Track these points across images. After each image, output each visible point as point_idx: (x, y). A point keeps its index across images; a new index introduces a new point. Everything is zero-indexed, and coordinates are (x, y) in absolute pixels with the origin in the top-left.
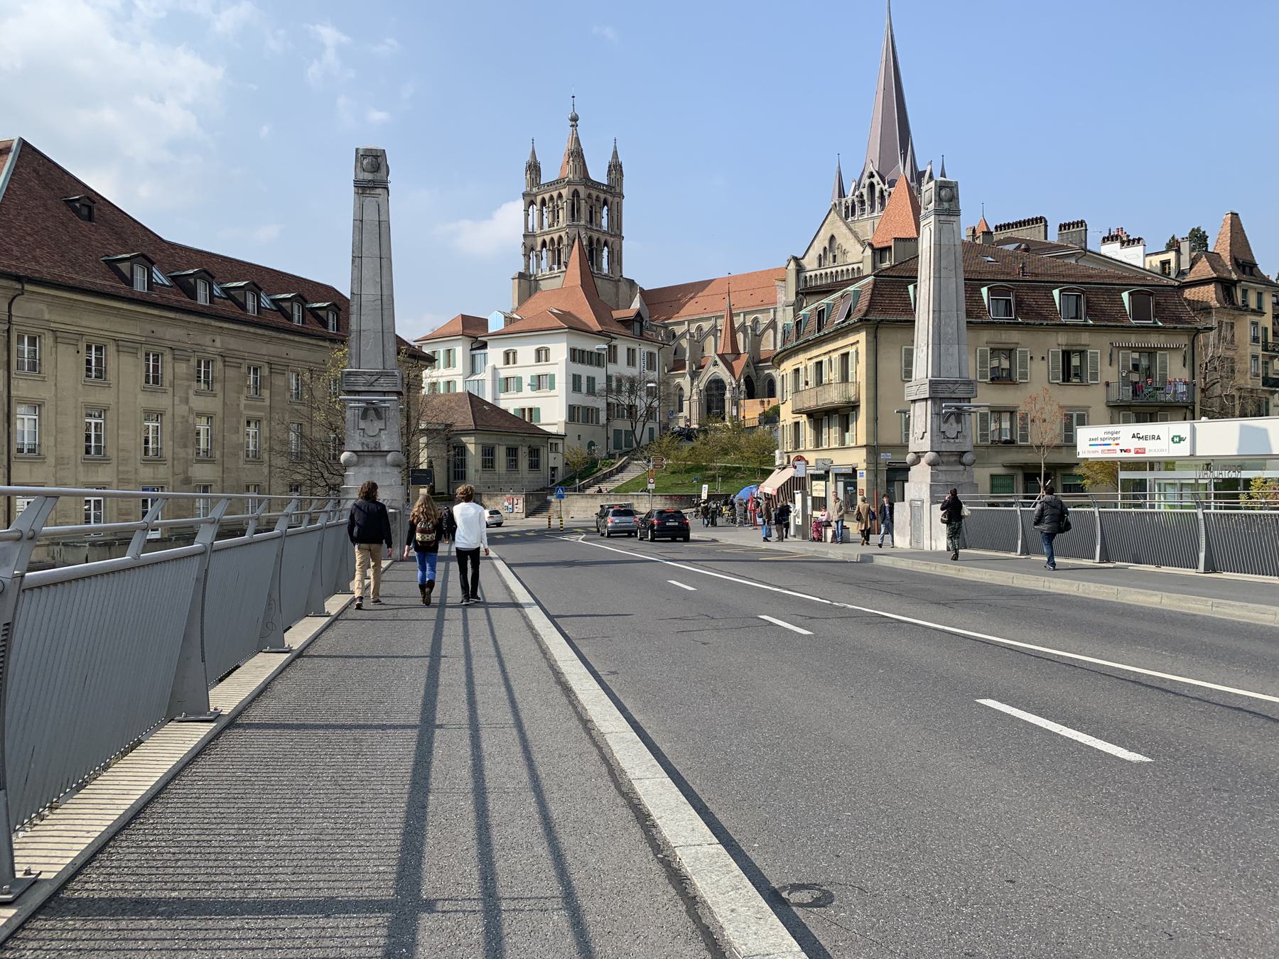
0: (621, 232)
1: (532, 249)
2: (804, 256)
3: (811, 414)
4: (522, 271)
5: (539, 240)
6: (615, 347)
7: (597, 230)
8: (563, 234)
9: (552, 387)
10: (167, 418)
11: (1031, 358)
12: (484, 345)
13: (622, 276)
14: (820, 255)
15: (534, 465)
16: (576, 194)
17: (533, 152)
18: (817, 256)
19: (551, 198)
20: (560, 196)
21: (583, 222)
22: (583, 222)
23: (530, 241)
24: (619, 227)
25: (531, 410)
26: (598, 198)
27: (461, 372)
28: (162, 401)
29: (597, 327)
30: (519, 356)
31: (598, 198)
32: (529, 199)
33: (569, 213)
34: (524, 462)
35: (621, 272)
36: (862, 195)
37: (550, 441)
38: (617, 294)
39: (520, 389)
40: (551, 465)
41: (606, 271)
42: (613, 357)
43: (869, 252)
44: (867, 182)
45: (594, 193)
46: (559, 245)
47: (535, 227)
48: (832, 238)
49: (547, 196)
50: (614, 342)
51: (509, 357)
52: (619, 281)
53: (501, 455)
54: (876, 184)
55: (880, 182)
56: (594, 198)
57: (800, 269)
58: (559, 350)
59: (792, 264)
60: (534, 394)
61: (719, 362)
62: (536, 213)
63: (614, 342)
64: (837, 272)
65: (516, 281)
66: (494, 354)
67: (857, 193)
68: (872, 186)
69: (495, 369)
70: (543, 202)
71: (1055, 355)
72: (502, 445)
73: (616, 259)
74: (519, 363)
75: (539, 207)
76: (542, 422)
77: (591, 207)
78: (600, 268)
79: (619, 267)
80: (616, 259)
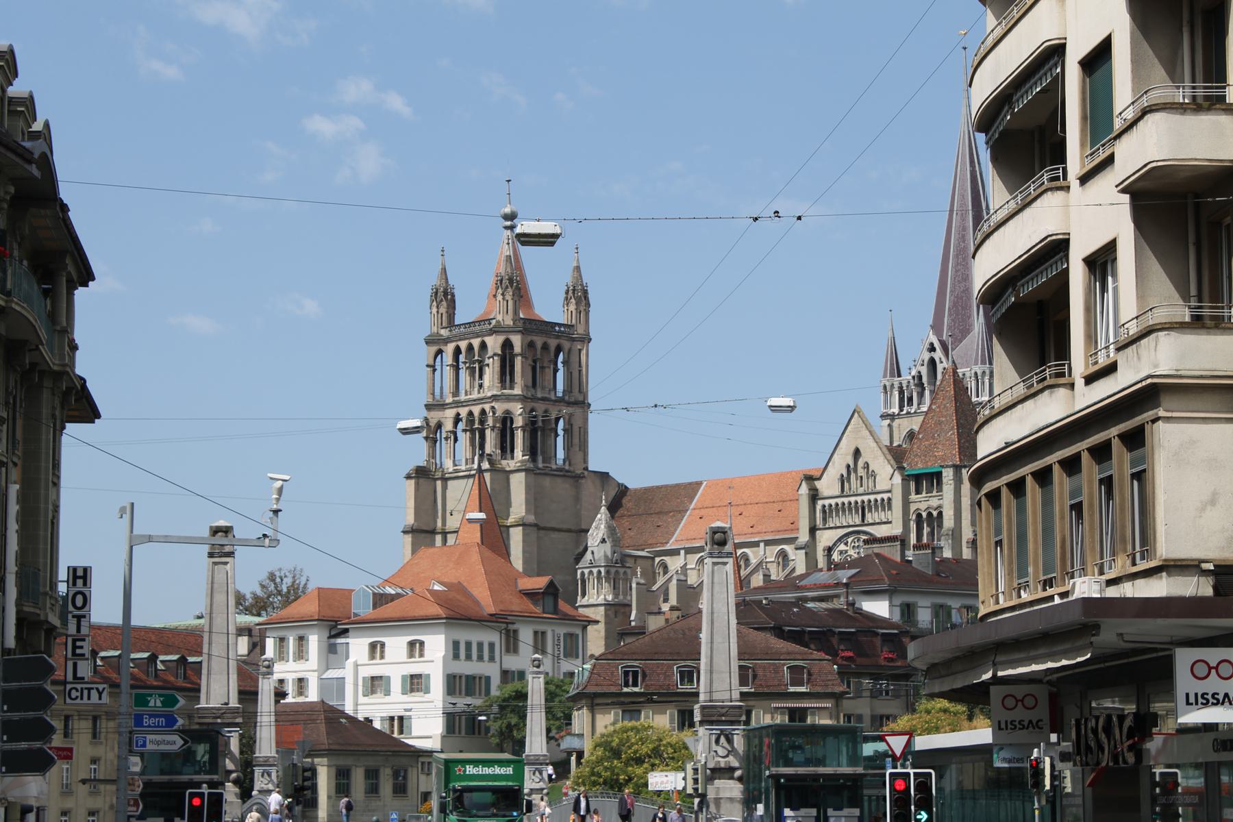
0: (585, 396)
1: (439, 426)
4: (423, 463)
5: (450, 413)
6: (515, 632)
7: (544, 399)
8: (487, 407)
9: (427, 691)
10: (102, 762)
12: (344, 632)
13: (586, 469)
14: (842, 476)
15: (400, 789)
16: (507, 345)
17: (444, 270)
18: (839, 476)
20: (483, 346)
21: (517, 391)
22: (517, 391)
23: (435, 416)
24: (583, 391)
25: (401, 718)
26: (545, 347)
27: (315, 668)
28: (99, 751)
29: (488, 605)
30: (387, 649)
31: (545, 347)
32: (434, 349)
33: (497, 376)
34: (386, 786)
35: (585, 461)
36: (920, 377)
37: (421, 759)
38: (577, 499)
39: (388, 693)
40: (423, 789)
41: (560, 462)
42: (512, 644)
43: (898, 479)
44: (926, 356)
45: (539, 341)
48: (857, 453)
49: (463, 345)
50: (511, 627)
51: (376, 650)
52: (581, 477)
53: (358, 779)
54: (938, 361)
55: (944, 359)
56: (539, 345)
57: (814, 496)
58: (436, 644)
59: (804, 489)
60: (406, 698)
63: (511, 627)
64: (863, 502)
65: (413, 482)
66: (358, 646)
67: (914, 373)
68: (932, 363)
69: (356, 665)
70: (457, 351)
72: (361, 766)
73: (576, 441)
74: (388, 658)
76: (414, 734)
77: (535, 361)
78: (550, 456)
79: (580, 455)
80: (578, 440)
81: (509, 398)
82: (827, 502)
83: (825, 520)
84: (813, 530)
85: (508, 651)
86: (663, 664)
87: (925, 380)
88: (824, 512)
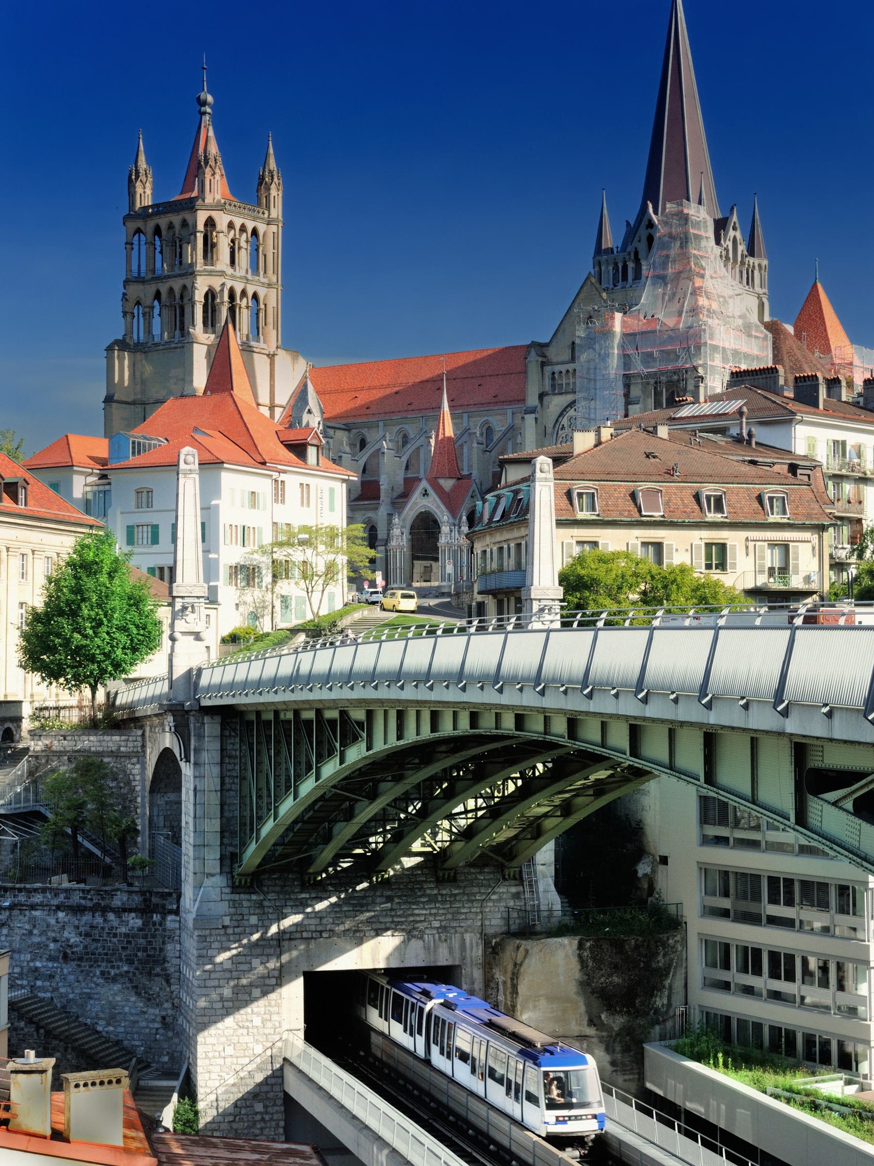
2: (551, 341)
3: (494, 593)
11: (677, 550)
19: (171, 226)
20: (184, 224)
23: (135, 291)
26: (243, 229)
31: (243, 229)
39: (155, 540)
46: (182, 297)
47: (143, 268)
61: (430, 491)
62: (143, 248)
70: (157, 231)
71: (699, 547)
75: (150, 238)
81: (211, 274)
82: (557, 368)
83: (553, 386)
84: (541, 396)
85: (276, 501)
86: (620, 486)
87: (640, 257)
88: (553, 379)
